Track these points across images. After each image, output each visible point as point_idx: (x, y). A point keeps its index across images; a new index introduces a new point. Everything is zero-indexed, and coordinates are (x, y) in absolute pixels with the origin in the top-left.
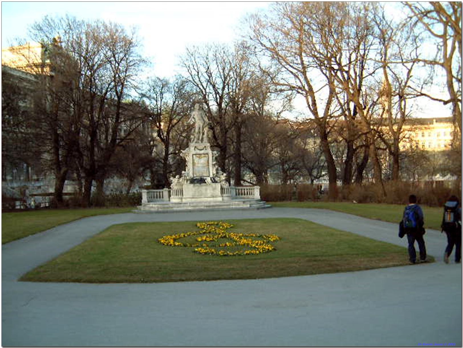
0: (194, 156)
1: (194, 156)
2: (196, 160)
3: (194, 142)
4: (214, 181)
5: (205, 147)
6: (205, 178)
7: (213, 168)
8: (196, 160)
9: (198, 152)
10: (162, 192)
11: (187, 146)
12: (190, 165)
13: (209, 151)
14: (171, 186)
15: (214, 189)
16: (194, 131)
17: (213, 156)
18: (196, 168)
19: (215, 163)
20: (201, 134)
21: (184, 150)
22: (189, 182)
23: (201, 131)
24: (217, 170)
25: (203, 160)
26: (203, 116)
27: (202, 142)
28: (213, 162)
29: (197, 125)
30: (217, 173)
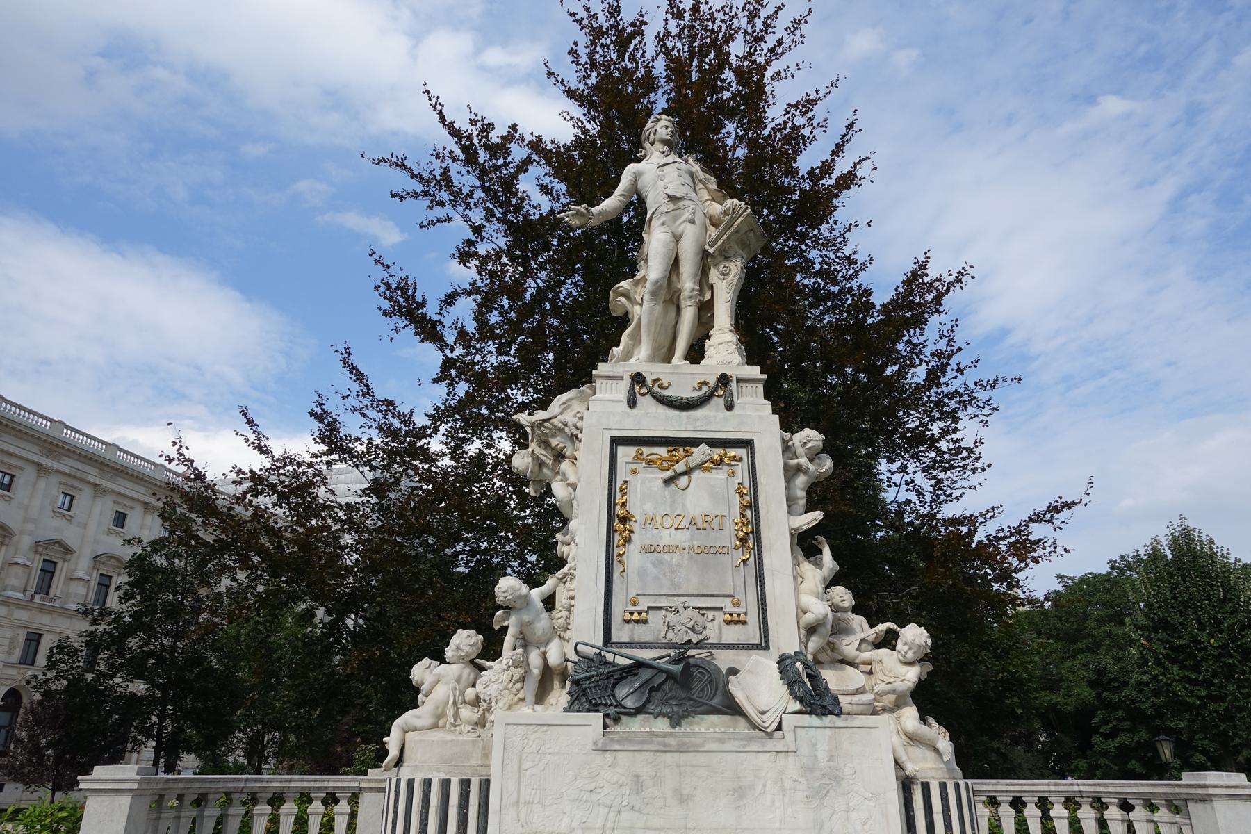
1: (622, 451)
2: (645, 489)
4: (816, 700)
5: (724, 380)
8: (645, 489)
9: (653, 419)
10: (354, 798)
11: (576, 372)
12: (583, 542)
13: (755, 416)
14: (392, 743)
15: (825, 783)
17: (791, 473)
18: (634, 557)
20: (689, 315)
22: (560, 696)
23: (687, 283)
25: (710, 493)
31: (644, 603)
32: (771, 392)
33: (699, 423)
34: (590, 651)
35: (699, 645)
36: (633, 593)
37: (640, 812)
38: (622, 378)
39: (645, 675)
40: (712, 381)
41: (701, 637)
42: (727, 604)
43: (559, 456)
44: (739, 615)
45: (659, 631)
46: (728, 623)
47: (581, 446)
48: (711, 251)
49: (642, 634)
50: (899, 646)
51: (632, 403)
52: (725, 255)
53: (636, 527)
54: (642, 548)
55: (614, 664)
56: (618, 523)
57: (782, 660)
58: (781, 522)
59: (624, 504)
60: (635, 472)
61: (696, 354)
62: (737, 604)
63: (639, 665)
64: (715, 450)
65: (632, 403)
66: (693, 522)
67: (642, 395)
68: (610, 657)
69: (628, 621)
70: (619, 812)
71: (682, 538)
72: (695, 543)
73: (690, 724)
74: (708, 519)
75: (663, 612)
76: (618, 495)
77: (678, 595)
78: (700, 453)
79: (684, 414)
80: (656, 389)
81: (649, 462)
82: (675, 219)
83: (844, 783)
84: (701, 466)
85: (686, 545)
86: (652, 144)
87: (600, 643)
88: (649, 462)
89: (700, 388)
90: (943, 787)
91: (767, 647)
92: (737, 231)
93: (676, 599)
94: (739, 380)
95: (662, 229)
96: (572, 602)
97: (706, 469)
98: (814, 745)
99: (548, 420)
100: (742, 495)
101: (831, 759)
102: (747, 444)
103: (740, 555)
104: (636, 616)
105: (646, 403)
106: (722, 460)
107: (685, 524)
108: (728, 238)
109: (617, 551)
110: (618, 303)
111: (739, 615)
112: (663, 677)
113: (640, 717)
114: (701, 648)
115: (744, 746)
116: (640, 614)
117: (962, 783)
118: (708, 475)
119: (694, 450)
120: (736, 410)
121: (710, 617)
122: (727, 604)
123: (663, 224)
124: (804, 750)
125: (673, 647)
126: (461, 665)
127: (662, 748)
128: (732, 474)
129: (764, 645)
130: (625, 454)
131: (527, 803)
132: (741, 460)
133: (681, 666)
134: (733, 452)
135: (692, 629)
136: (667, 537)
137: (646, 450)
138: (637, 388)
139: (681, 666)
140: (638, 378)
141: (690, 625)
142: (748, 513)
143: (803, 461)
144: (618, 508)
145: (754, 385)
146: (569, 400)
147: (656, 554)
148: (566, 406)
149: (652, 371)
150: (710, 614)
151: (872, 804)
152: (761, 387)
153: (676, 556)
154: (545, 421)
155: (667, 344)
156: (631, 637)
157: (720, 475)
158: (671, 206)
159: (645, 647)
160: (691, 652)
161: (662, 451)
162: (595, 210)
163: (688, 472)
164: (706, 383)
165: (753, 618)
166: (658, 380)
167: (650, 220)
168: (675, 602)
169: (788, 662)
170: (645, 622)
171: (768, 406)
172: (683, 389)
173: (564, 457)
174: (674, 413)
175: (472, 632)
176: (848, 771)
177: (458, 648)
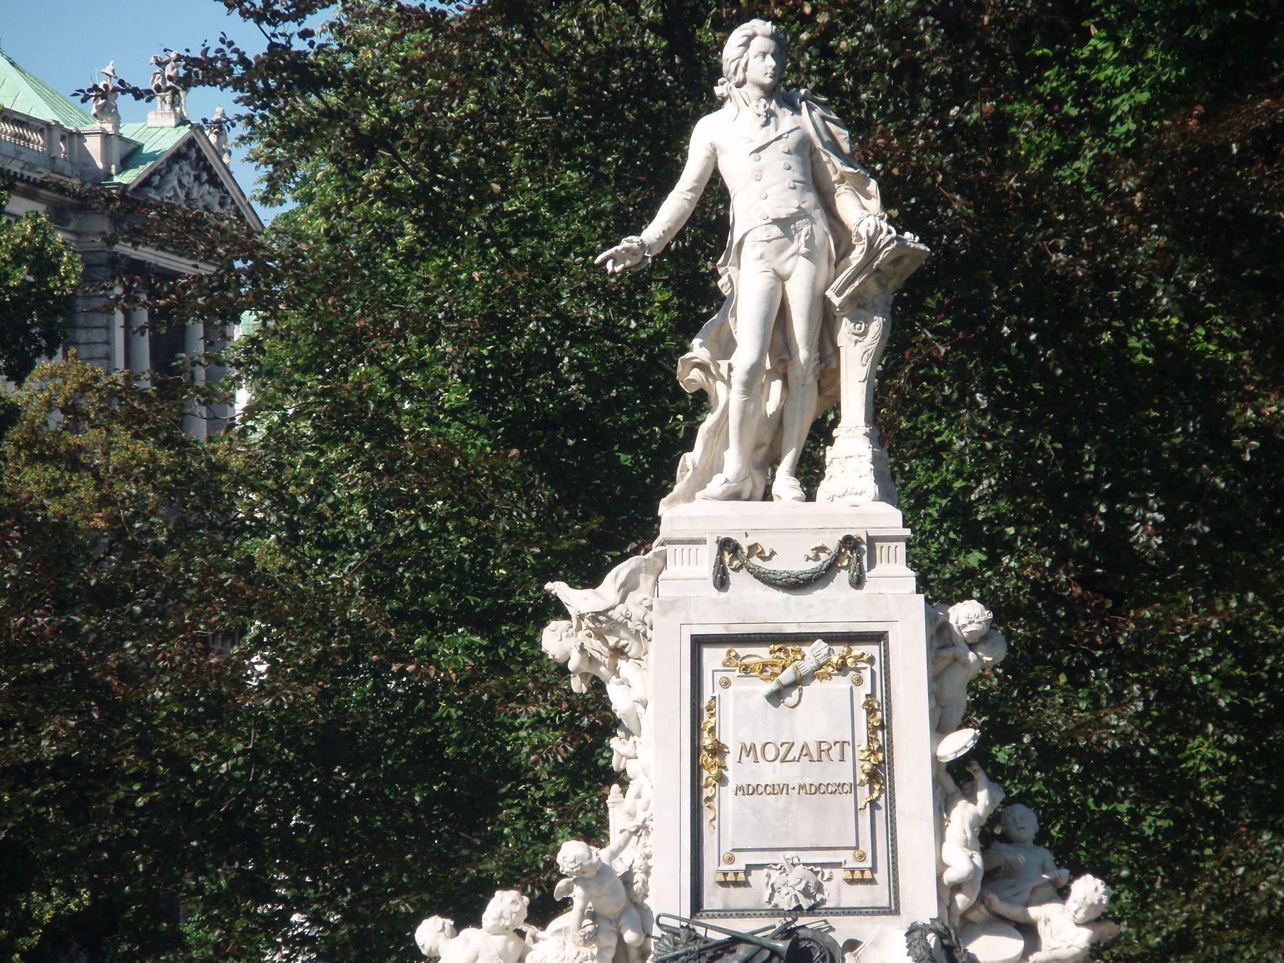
0: (713, 657)
2: (740, 707)
3: (717, 485)
5: (850, 543)
6: (843, 929)
7: (943, 805)
8: (740, 707)
12: (650, 761)
16: (726, 347)
19: (960, 742)
21: (590, 578)
24: (988, 835)
25: (828, 709)
26: (835, 166)
27: (810, 497)
28: (940, 728)
29: (746, 281)
30: (992, 876)
31: (742, 861)
32: (912, 562)
34: (675, 924)
35: (812, 910)
36: (727, 848)
38: (702, 541)
39: (742, 951)
40: (833, 546)
42: (847, 857)
43: (619, 652)
44: (862, 872)
45: (761, 895)
46: (852, 882)
47: (652, 647)
48: (836, 301)
49: (739, 898)
50: (1070, 902)
51: (722, 582)
52: (859, 307)
53: (730, 760)
55: (706, 941)
56: (704, 756)
57: (914, 931)
58: (918, 751)
59: (712, 730)
60: (726, 684)
61: (810, 473)
63: (736, 940)
64: (839, 649)
65: (722, 582)
67: (736, 570)
68: (700, 931)
69: (724, 884)
71: (790, 773)
72: (808, 781)
74: (824, 747)
75: (766, 871)
76: (706, 714)
77: (785, 849)
78: (814, 652)
79: (794, 599)
80: (756, 561)
81: (746, 670)
82: (781, 250)
85: (794, 783)
86: (739, 85)
87: (686, 913)
88: (746, 670)
89: (817, 558)
91: (896, 912)
92: (878, 270)
93: (781, 854)
94: (872, 541)
95: (760, 266)
96: (650, 862)
99: (608, 610)
100: (871, 711)
102: (878, 638)
103: (864, 793)
104: (730, 878)
106: (844, 664)
107: (795, 752)
108: (861, 284)
109: (707, 793)
110: (689, 378)
111: (862, 872)
112: (767, 954)
114: (814, 915)
116: (736, 874)
118: (826, 684)
119: (806, 649)
120: (869, 587)
122: (847, 857)
123: (762, 257)
125: (779, 915)
126: (502, 938)
128: (859, 681)
130: (713, 657)
132: (871, 660)
133: (788, 942)
134: (857, 650)
136: (770, 773)
137: (741, 651)
138: (727, 557)
139: (788, 942)
140: (727, 545)
141: (802, 886)
142: (880, 733)
144: (705, 734)
145: (893, 545)
146: (633, 575)
147: (756, 795)
148: (628, 587)
149: (744, 520)
150: (827, 871)
152: (902, 546)
154: (598, 613)
155: (767, 439)
157: (841, 684)
158: (776, 231)
159: (743, 916)
160: (801, 921)
161: (763, 653)
162: (654, 231)
163: (799, 682)
164: (822, 549)
165: (882, 875)
166: (756, 545)
167: (741, 244)
168: (779, 858)
169: (917, 934)
170: (745, 884)
171: (910, 578)
172: (794, 562)
173: (626, 654)
174: (780, 595)
175: (512, 894)
177: (501, 917)
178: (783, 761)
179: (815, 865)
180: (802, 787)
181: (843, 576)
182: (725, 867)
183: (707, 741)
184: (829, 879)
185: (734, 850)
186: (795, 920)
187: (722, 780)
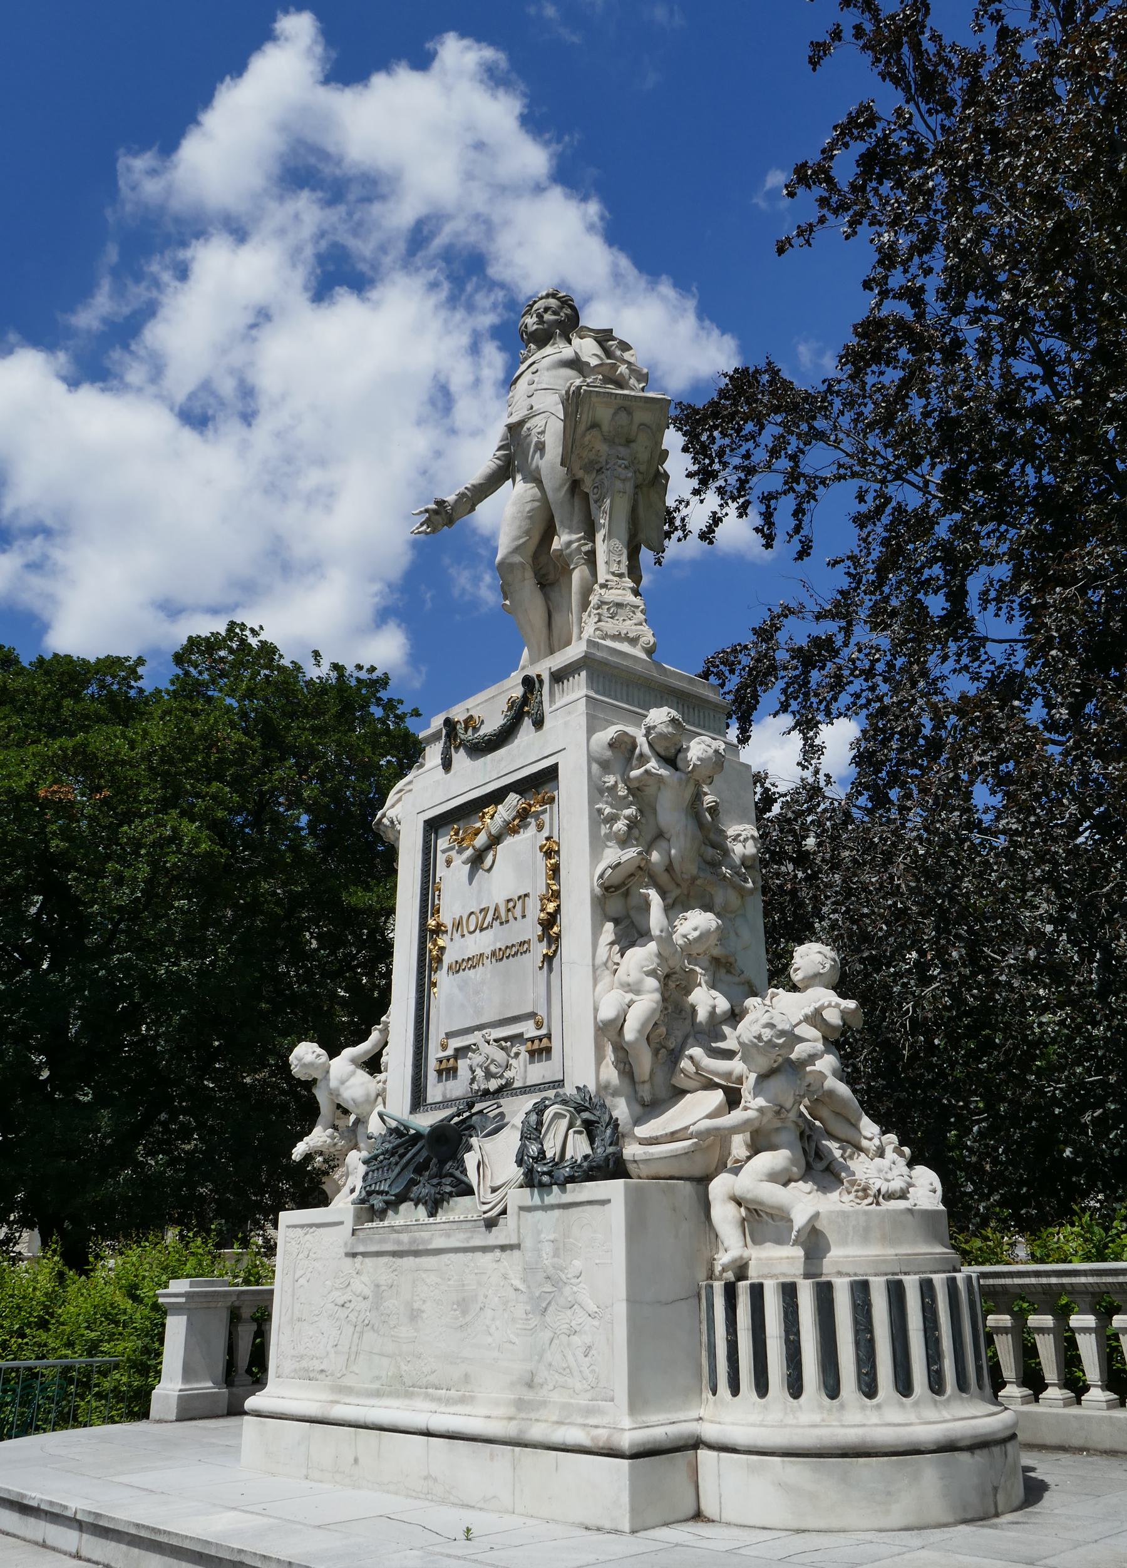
33: (503, 764)
37: (377, 1332)
40: (518, 692)
41: (503, 1082)
54: (450, 968)
60: (449, 862)
62: (539, 1026)
66: (496, 918)
70: (362, 1333)
72: (498, 945)
73: (446, 1212)
83: (567, 1290)
84: (510, 829)
85: (488, 952)
90: (789, 1292)
97: (515, 831)
98: (539, 1232)
101: (556, 1254)
104: (443, 1066)
105: (460, 758)
113: (403, 1207)
115: (468, 1239)
117: (911, 1284)
121: (514, 1050)
124: (528, 1243)
127: (395, 1248)
129: (560, 1083)
131: (299, 1320)
135: (489, 1075)
143: (653, 765)
151: (596, 1323)
153: (480, 969)
156: (444, 1096)
163: (495, 840)
166: (471, 717)
172: (492, 724)
176: (572, 1272)
178: (482, 930)
179: (505, 1039)
180: (494, 954)
181: (527, 722)
182: (442, 1054)
183: (432, 923)
184: (517, 1055)
185: (449, 1035)
186: (471, 1106)
187: (439, 960)
